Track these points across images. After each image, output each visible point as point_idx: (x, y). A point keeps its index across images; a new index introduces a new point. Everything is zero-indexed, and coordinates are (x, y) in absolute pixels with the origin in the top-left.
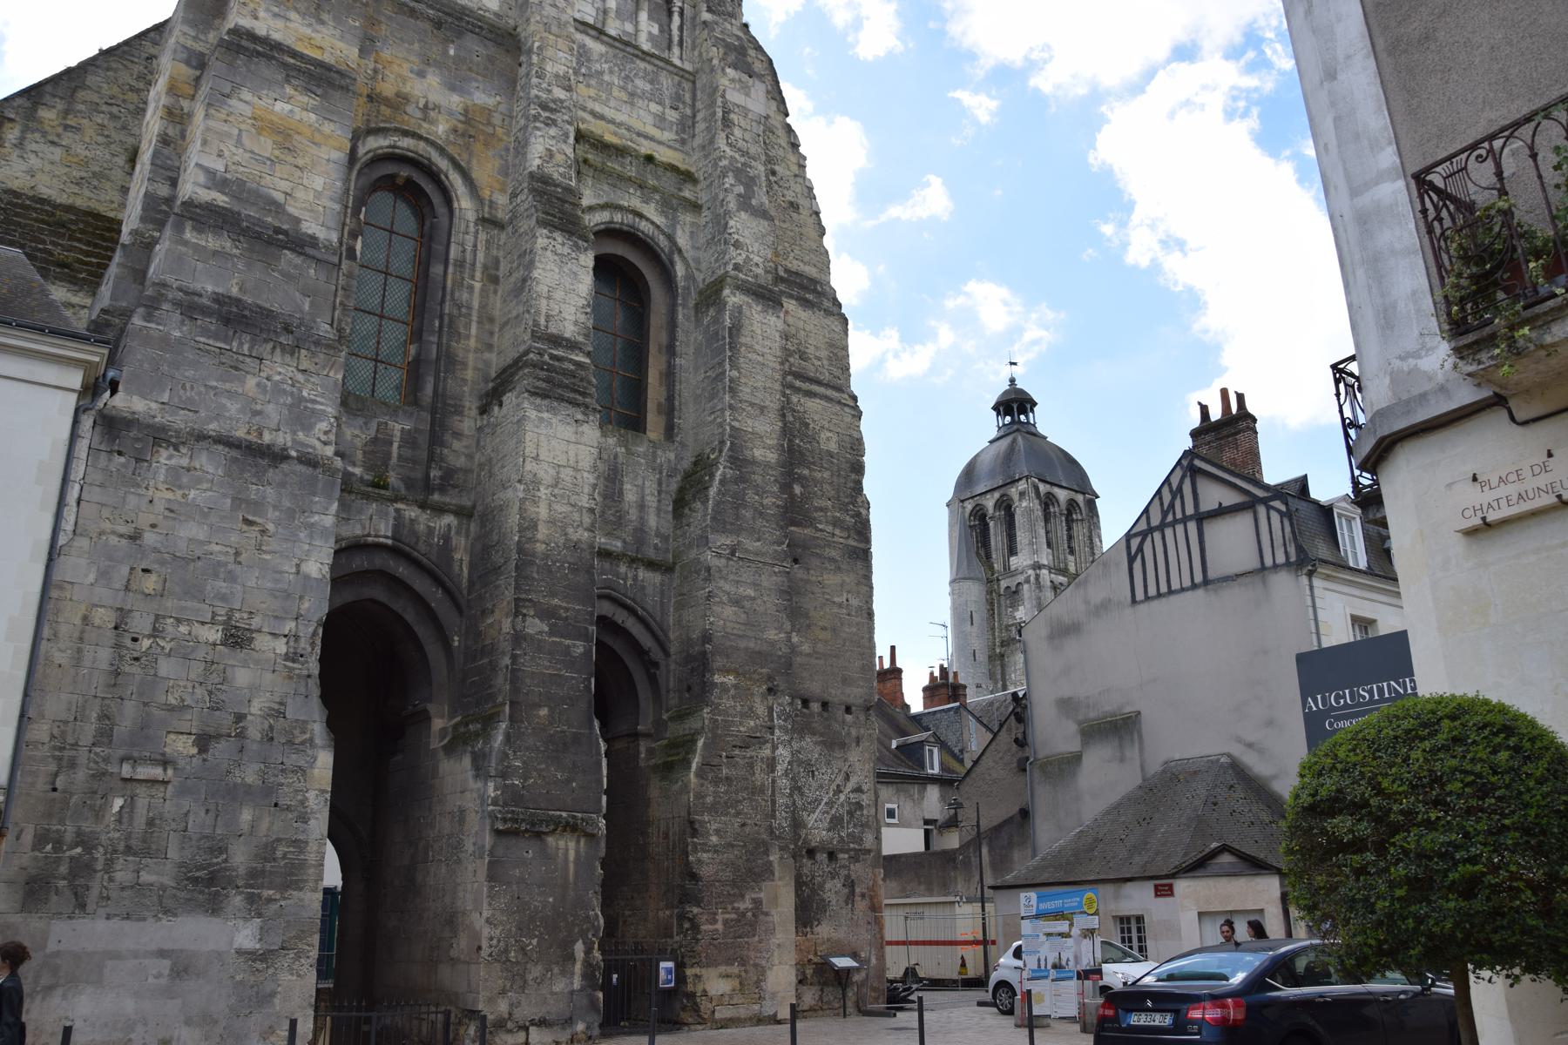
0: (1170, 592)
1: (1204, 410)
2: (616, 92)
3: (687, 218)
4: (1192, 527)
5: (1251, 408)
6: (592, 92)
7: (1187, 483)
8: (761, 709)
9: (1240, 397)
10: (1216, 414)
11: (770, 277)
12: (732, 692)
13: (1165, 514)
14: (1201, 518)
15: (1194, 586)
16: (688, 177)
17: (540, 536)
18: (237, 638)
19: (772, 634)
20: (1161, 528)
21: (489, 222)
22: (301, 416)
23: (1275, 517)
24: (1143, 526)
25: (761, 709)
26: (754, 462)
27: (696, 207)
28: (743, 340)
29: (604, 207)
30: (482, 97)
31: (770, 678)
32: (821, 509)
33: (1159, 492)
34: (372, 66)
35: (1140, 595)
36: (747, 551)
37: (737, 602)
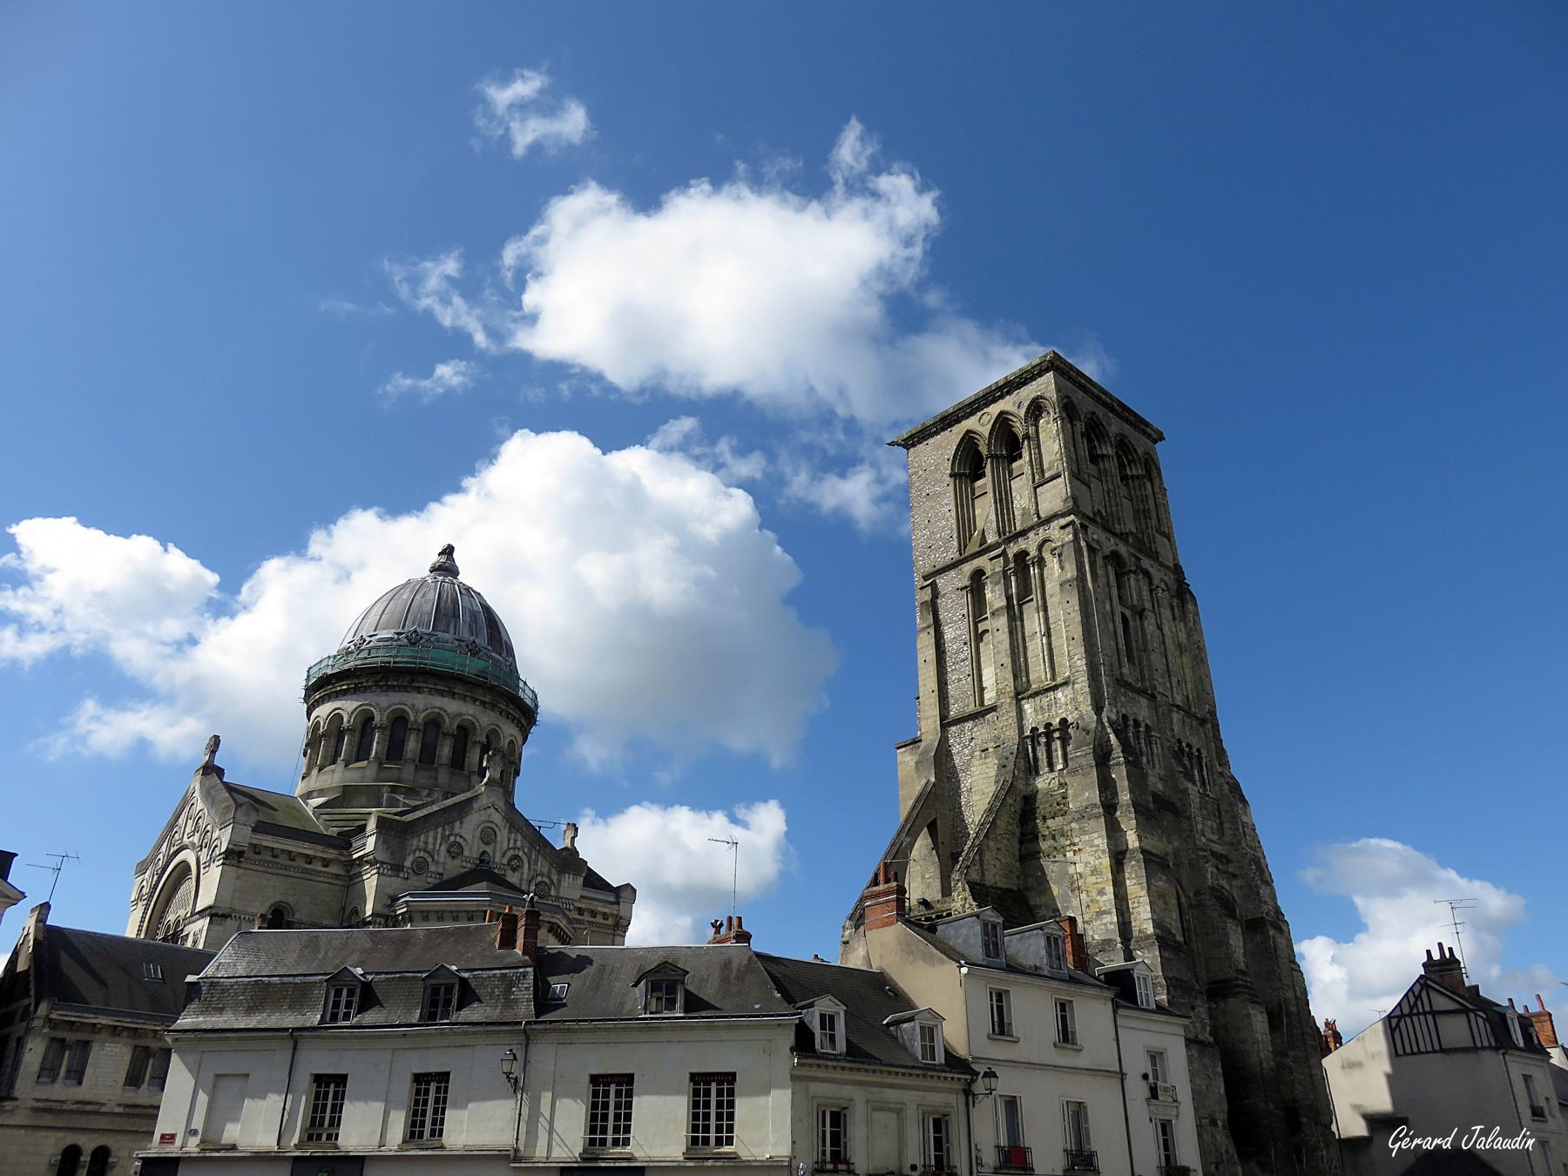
0: (1420, 1052)
1: (1428, 952)
3: (1235, 883)
4: (1430, 1017)
5: (1458, 956)
7: (1424, 995)
9: (1450, 949)
10: (1436, 956)
13: (1411, 1008)
14: (1434, 1013)
15: (1434, 1051)
16: (1225, 859)
18: (1213, 1123)
20: (1410, 1015)
21: (1190, 906)
22: (1204, 1026)
23: (1480, 1021)
24: (1398, 1013)
27: (1235, 876)
30: (1176, 844)
33: (1406, 995)
35: (1400, 1052)
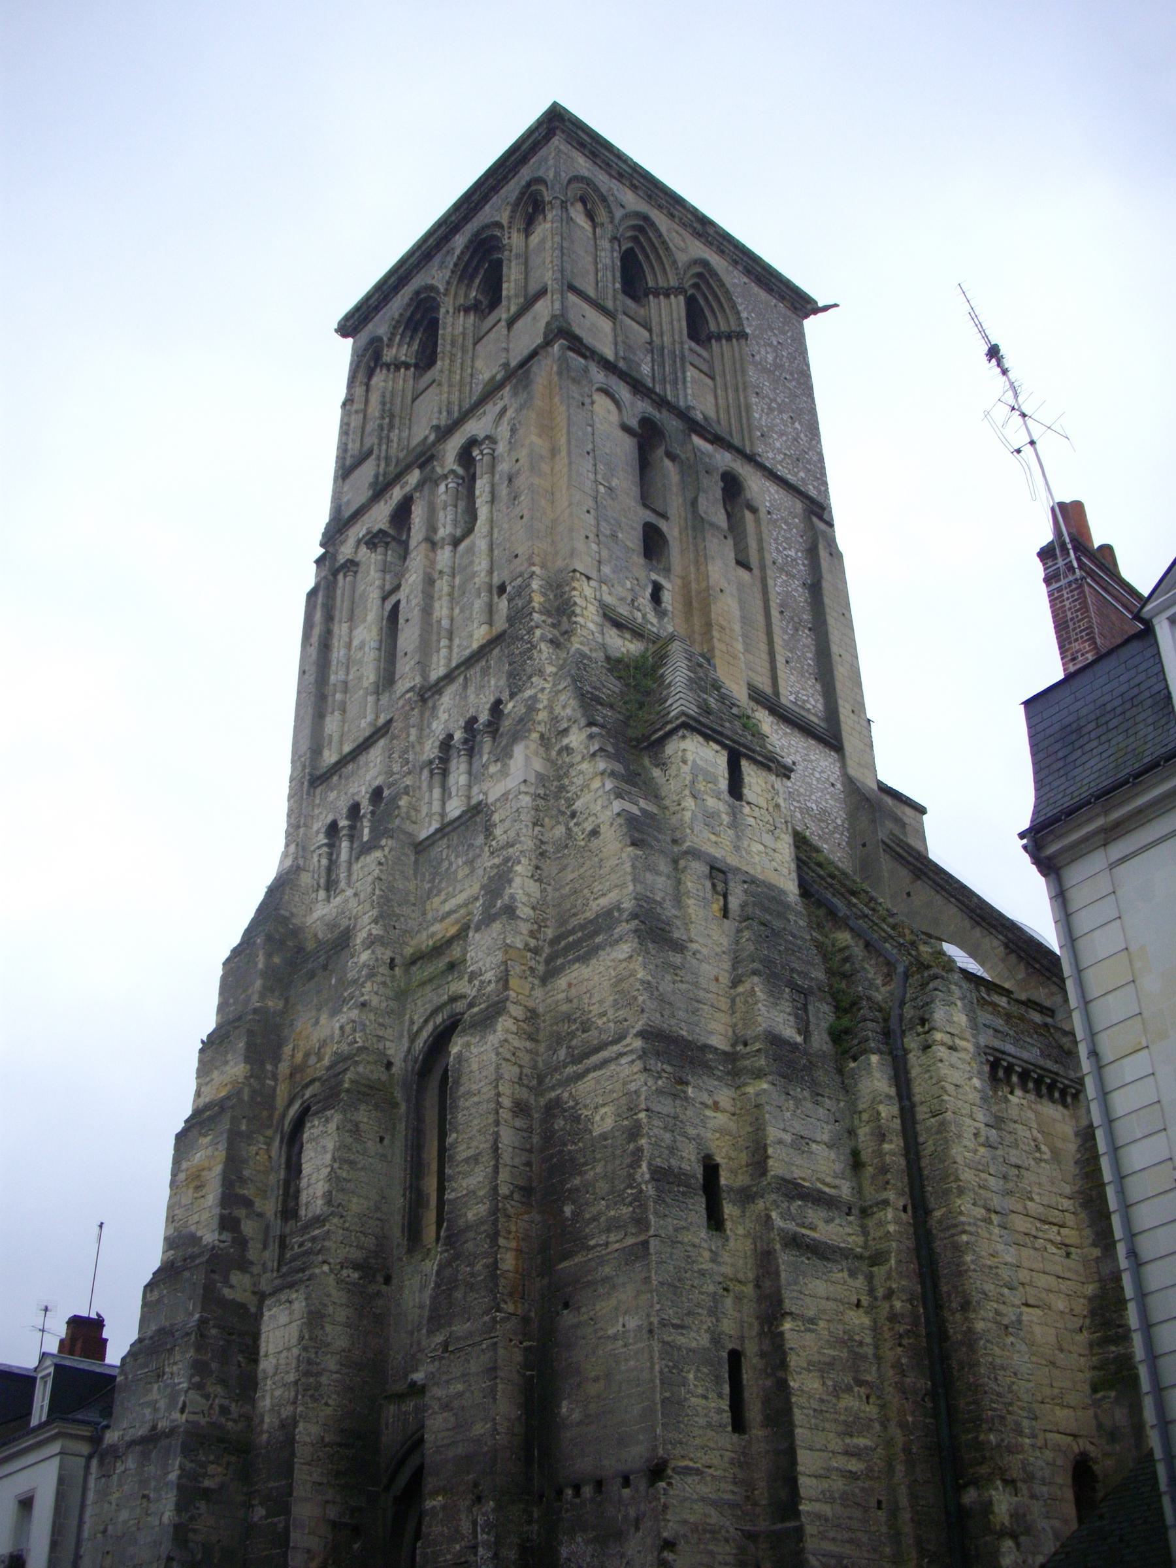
2: (460, 875)
6: (443, 896)
8: (465, 1527)
11: (500, 986)
12: (441, 1515)
17: (265, 1427)
19: (479, 1429)
25: (465, 1527)
26: (468, 1228)
28: (462, 1090)
29: (426, 1021)
31: (476, 1485)
32: (595, 1219)
34: (291, 1046)
36: (458, 1339)
37: (446, 1407)
